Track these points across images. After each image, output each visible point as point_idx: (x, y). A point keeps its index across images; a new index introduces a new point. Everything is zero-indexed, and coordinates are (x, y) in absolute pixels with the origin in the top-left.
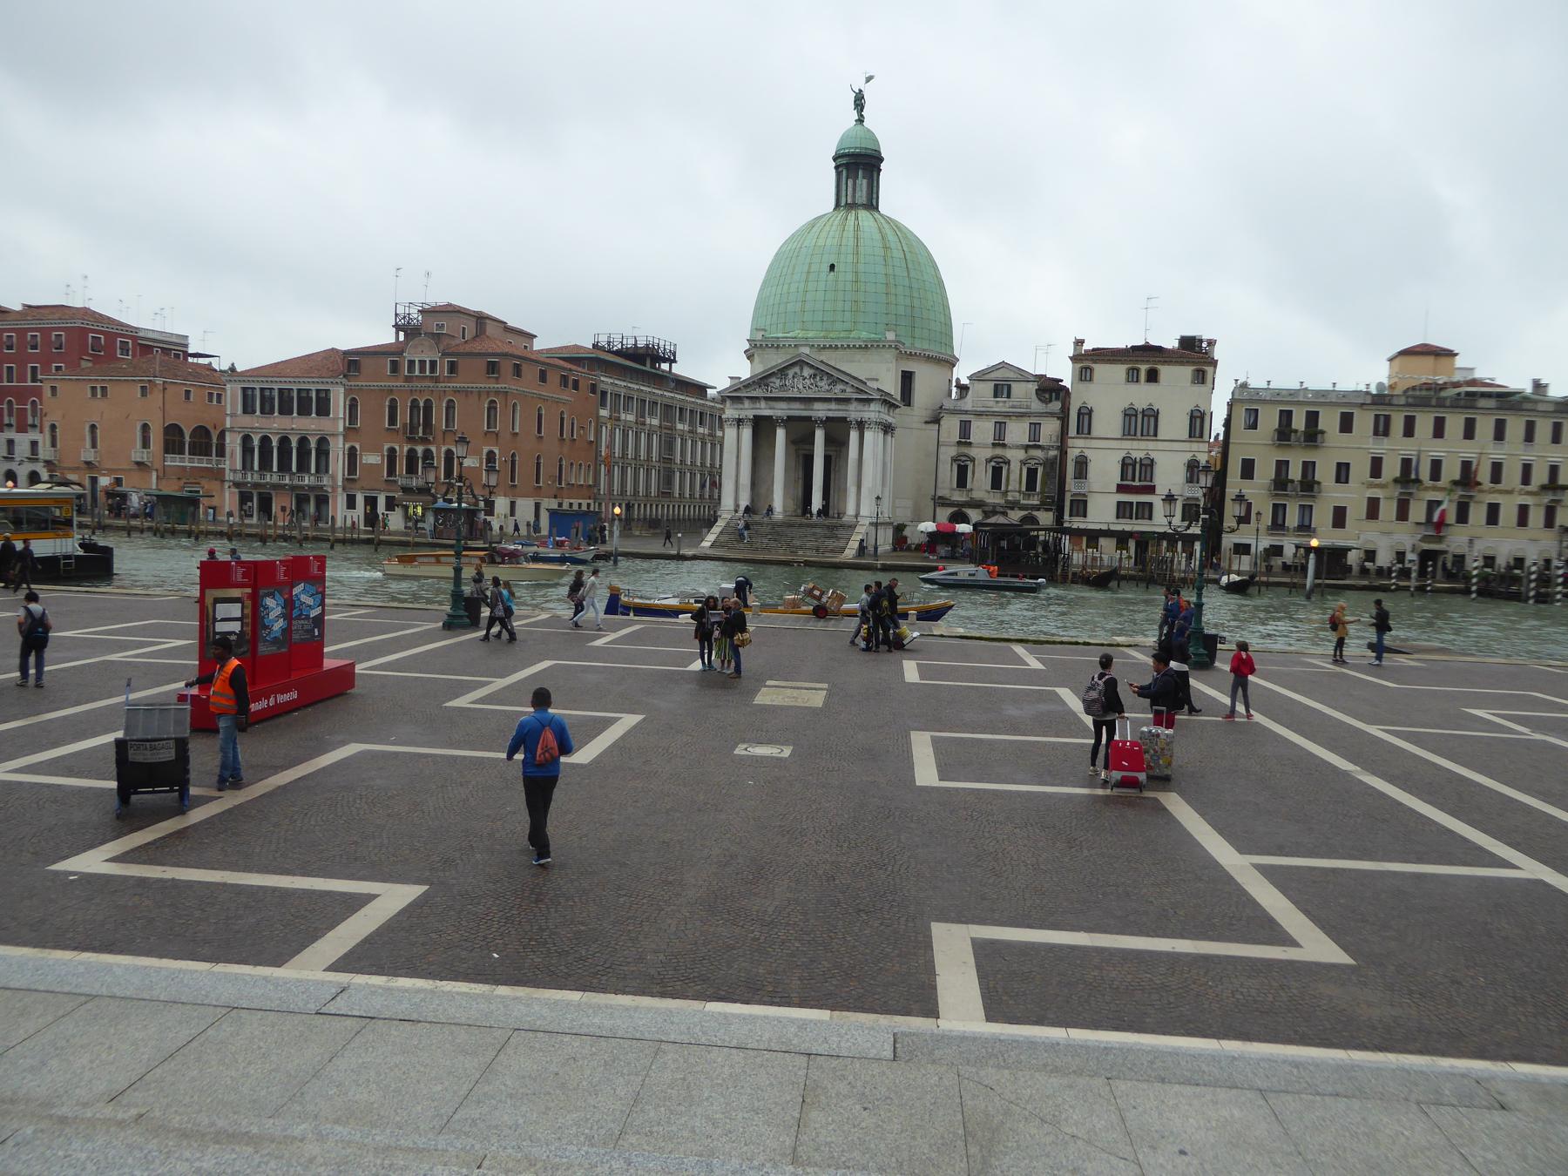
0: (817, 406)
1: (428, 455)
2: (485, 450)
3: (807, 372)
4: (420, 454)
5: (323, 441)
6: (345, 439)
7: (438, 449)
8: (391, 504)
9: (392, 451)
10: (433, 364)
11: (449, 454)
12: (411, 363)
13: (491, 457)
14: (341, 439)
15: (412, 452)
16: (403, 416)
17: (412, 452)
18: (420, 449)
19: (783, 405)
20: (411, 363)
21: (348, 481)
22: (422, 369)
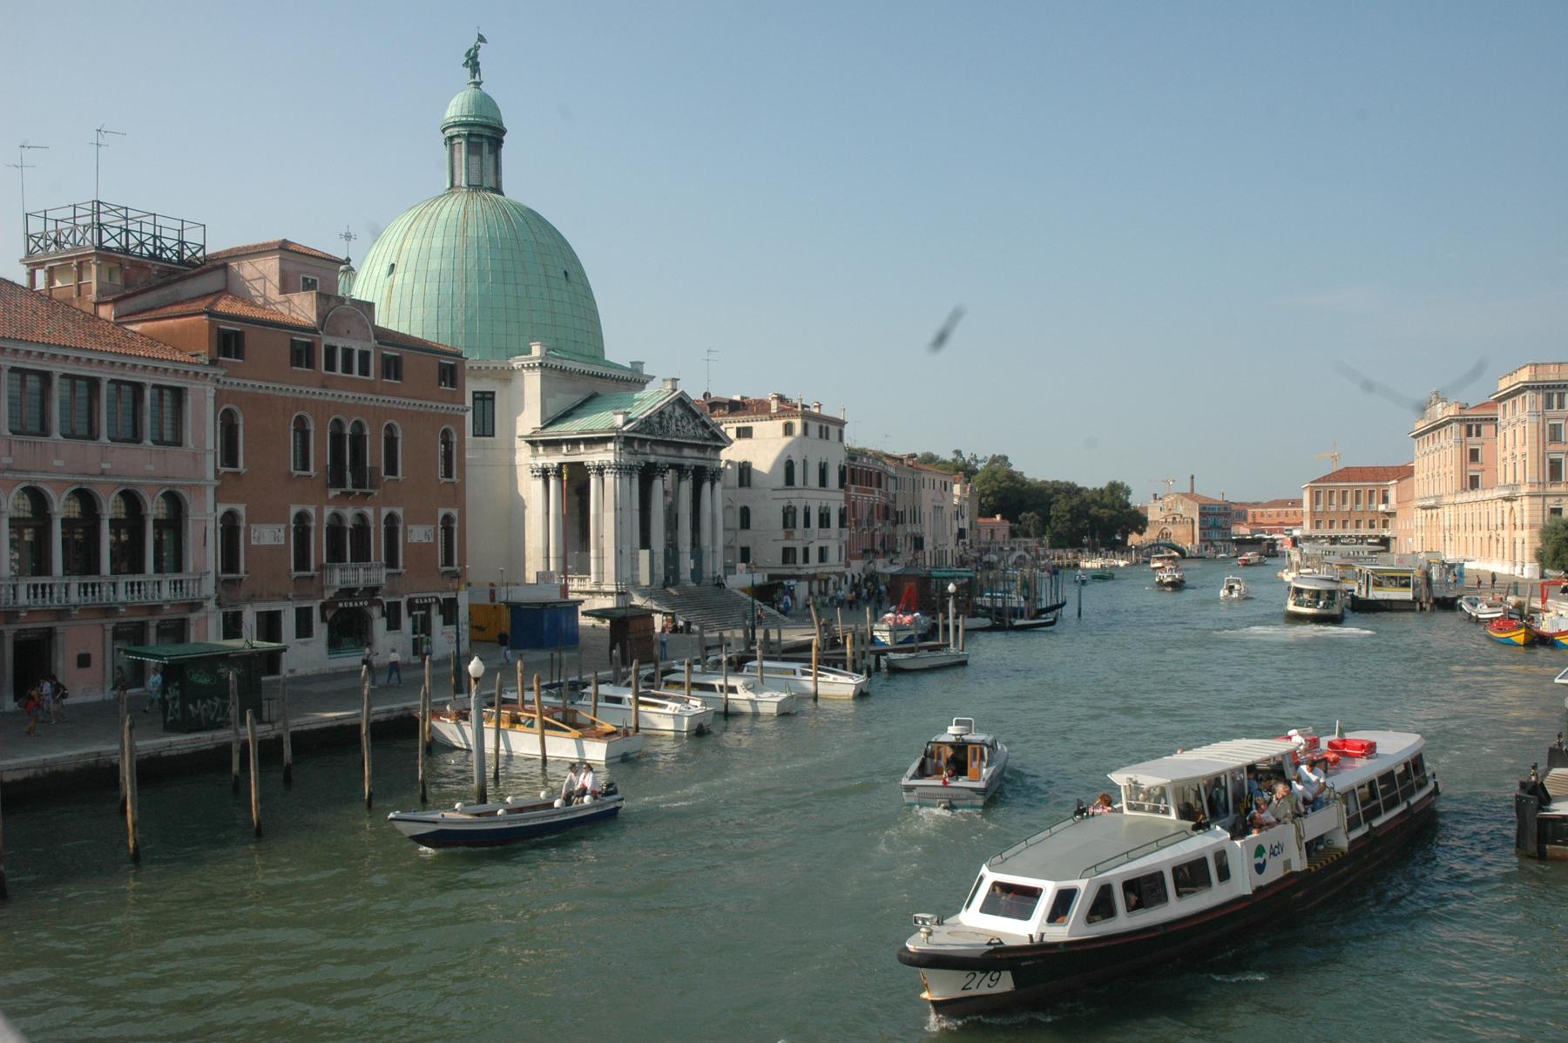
0: (687, 452)
1: (362, 529)
2: (441, 513)
3: (679, 411)
4: (349, 525)
5: (174, 500)
6: (218, 499)
7: (377, 514)
8: (304, 629)
9: (302, 518)
10: (365, 356)
11: (391, 519)
12: (330, 351)
13: (447, 519)
14: (210, 493)
15: (337, 517)
16: (319, 452)
17: (337, 517)
18: (349, 514)
19: (662, 450)
20: (330, 351)
21: (228, 586)
22: (348, 368)
